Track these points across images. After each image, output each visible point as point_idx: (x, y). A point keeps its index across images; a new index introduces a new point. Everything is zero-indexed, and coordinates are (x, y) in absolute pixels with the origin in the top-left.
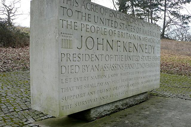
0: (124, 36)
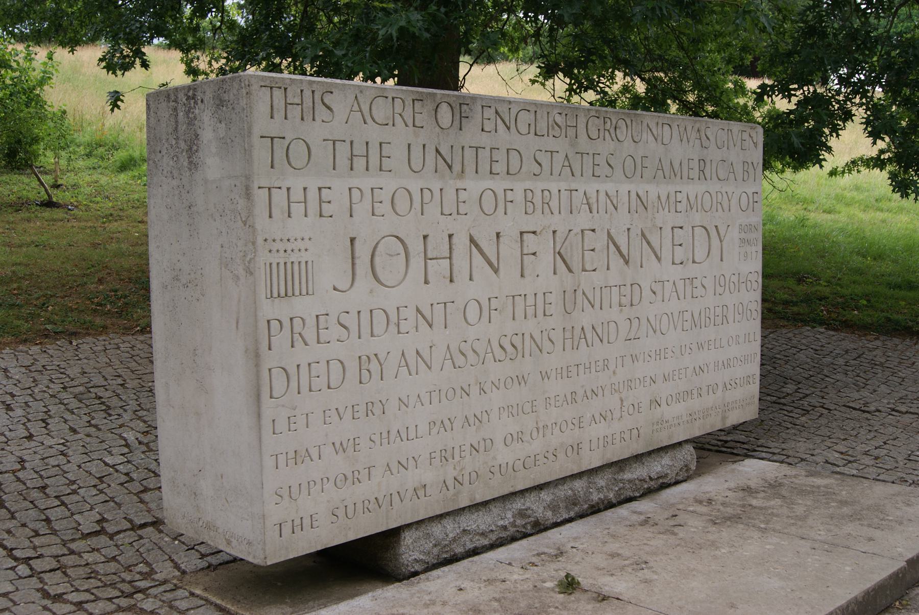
0: (554, 204)
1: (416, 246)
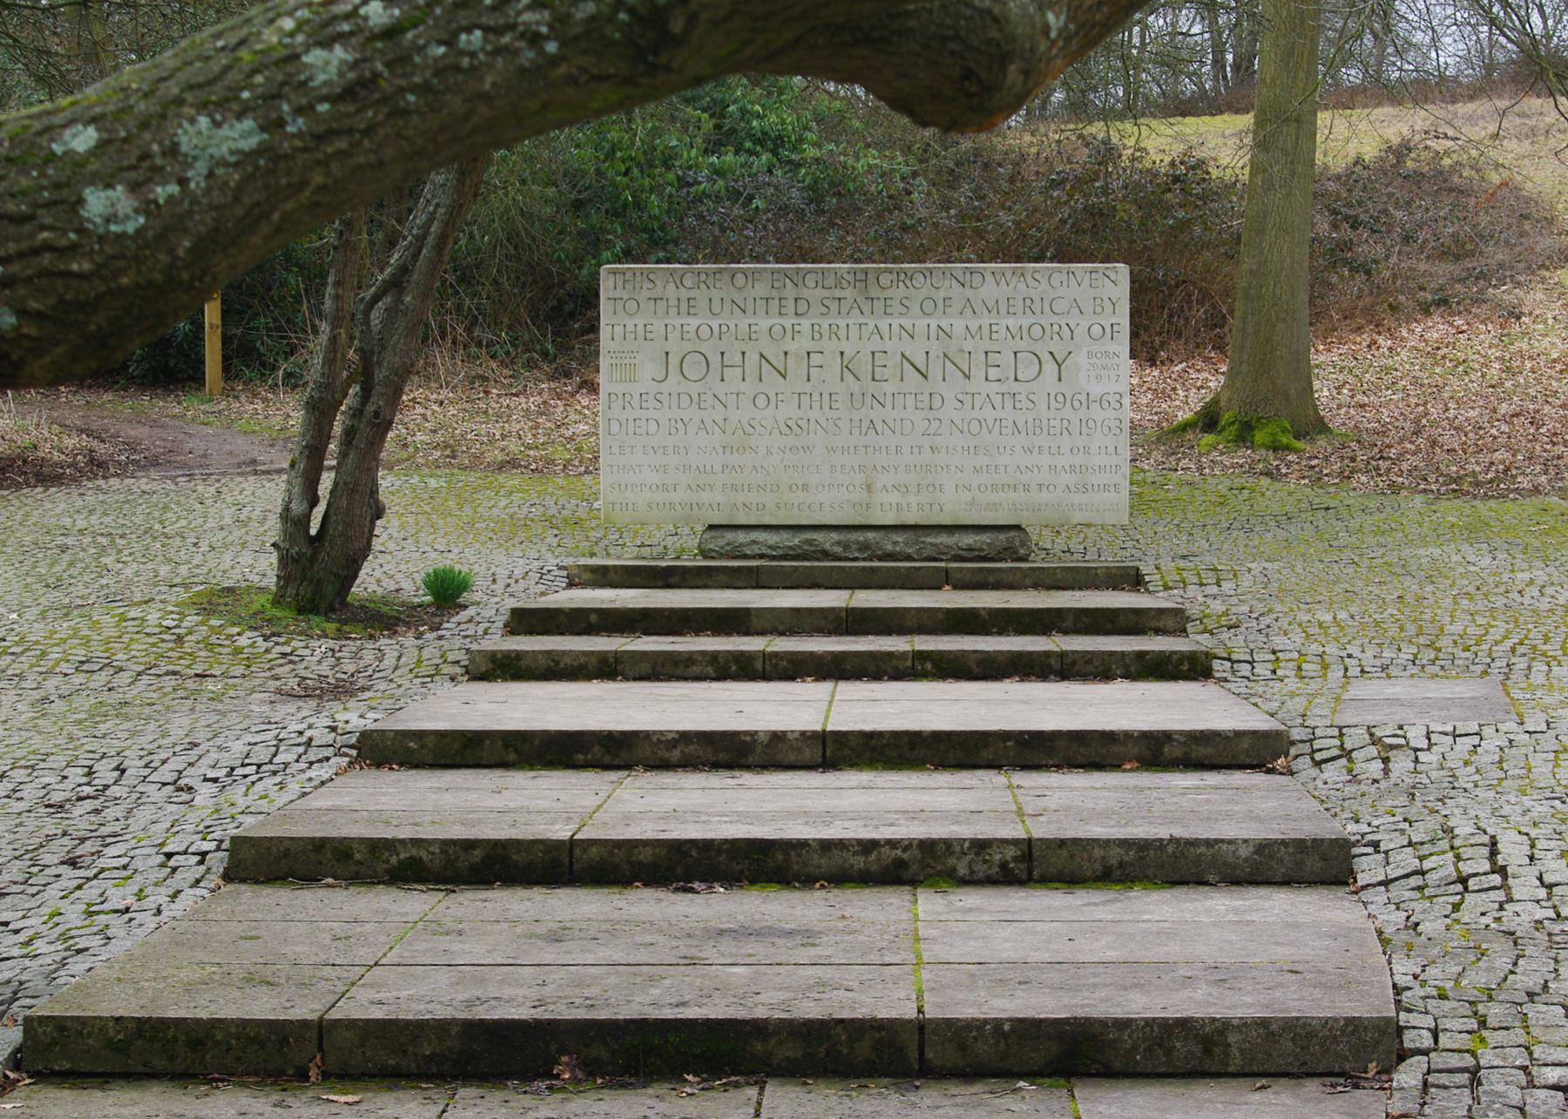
0: (842, 333)
1: (715, 360)
